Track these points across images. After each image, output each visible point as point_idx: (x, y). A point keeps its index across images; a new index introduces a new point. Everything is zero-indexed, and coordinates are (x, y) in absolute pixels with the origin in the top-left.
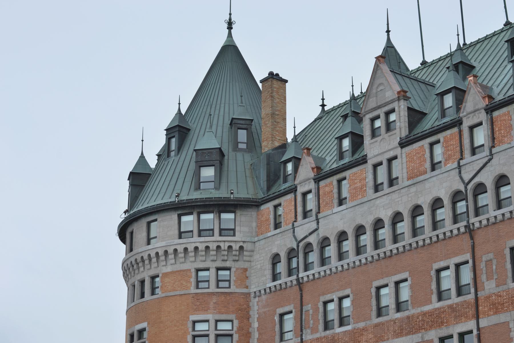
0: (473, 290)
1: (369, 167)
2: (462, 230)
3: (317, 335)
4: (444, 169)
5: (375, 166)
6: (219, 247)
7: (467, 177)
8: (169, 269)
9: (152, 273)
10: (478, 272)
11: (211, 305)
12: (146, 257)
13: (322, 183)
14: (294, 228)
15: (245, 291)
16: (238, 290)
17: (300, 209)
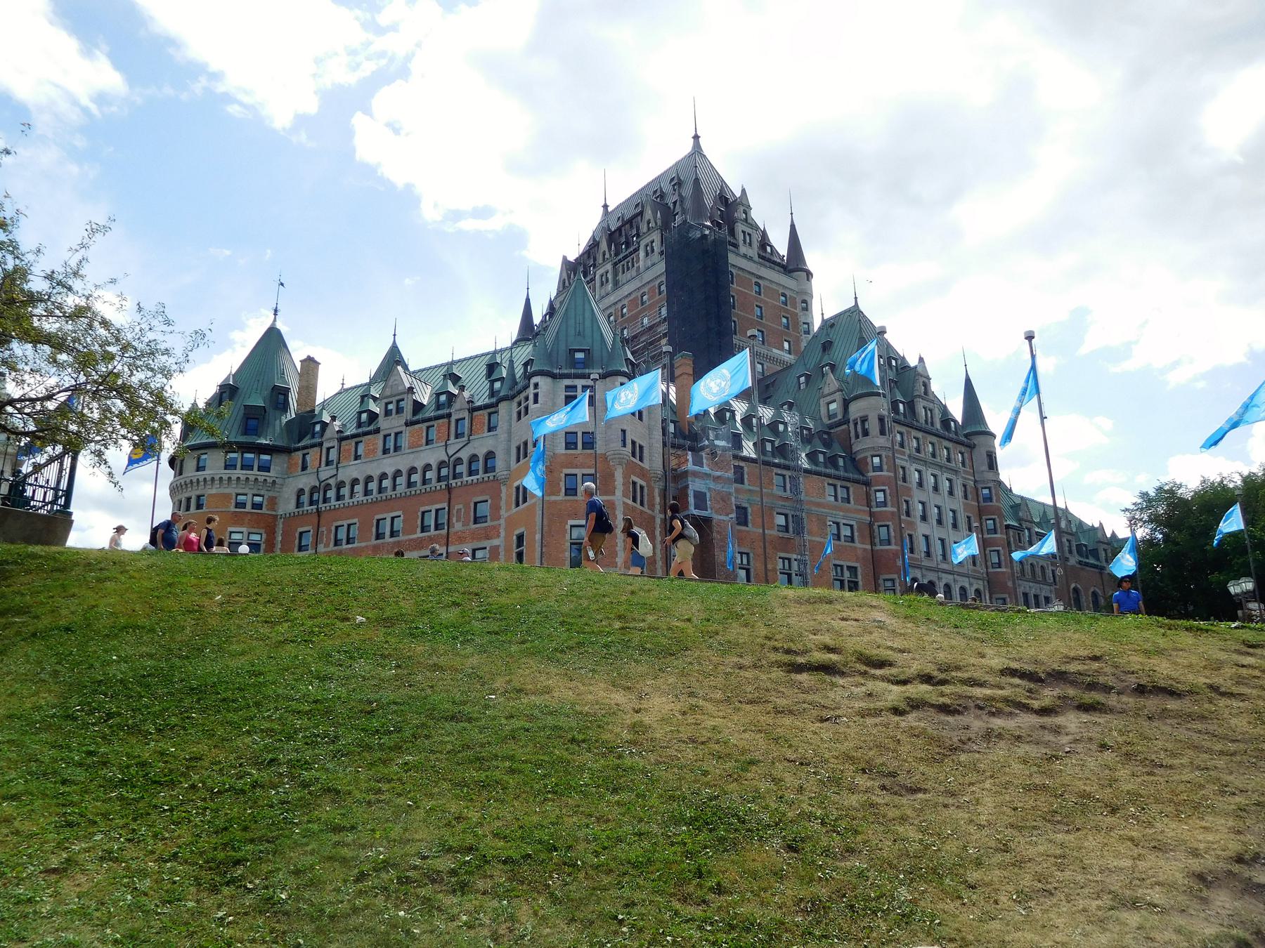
0: (446, 527)
1: (381, 436)
2: (444, 487)
3: (329, 549)
4: (435, 445)
5: (385, 437)
6: (256, 479)
7: (450, 454)
8: (214, 491)
9: (198, 493)
10: (451, 515)
11: (246, 521)
12: (195, 480)
13: (344, 443)
14: (318, 472)
15: (274, 513)
16: (267, 512)
17: (324, 459)
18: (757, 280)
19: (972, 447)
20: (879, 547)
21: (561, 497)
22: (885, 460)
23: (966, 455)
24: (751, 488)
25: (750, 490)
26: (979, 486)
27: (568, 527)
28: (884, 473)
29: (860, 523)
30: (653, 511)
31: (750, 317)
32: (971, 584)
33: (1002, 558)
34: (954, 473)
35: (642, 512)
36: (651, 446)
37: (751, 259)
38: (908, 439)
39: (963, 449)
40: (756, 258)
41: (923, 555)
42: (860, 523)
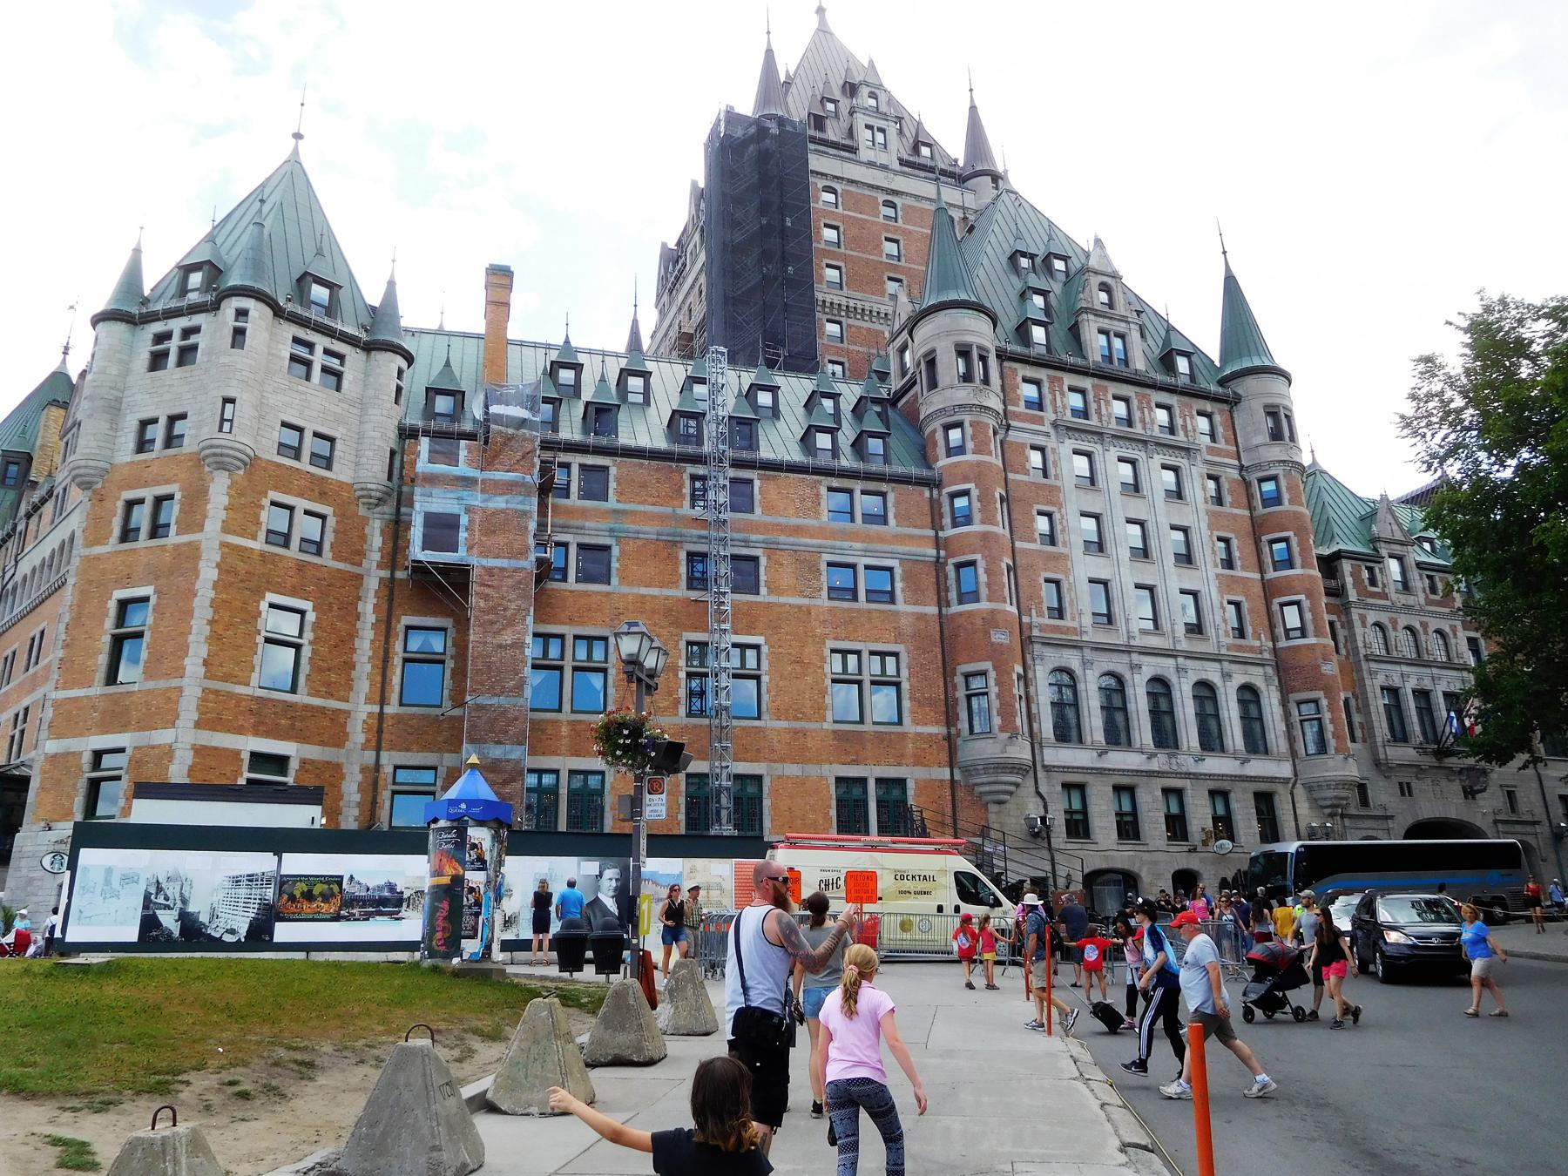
18: (889, 198)
19: (1232, 402)
20: (956, 608)
21: (112, 544)
22: (969, 430)
23: (1217, 418)
24: (621, 506)
25: (616, 512)
26: (1253, 477)
27: (112, 606)
28: (969, 457)
29: (909, 562)
30: (360, 564)
31: (871, 257)
32: (1226, 676)
33: (1308, 616)
34: (1183, 454)
35: (301, 567)
36: (361, 437)
37: (884, 168)
38: (1053, 392)
39: (1208, 407)
40: (896, 165)
41: (1087, 621)
42: (909, 562)
